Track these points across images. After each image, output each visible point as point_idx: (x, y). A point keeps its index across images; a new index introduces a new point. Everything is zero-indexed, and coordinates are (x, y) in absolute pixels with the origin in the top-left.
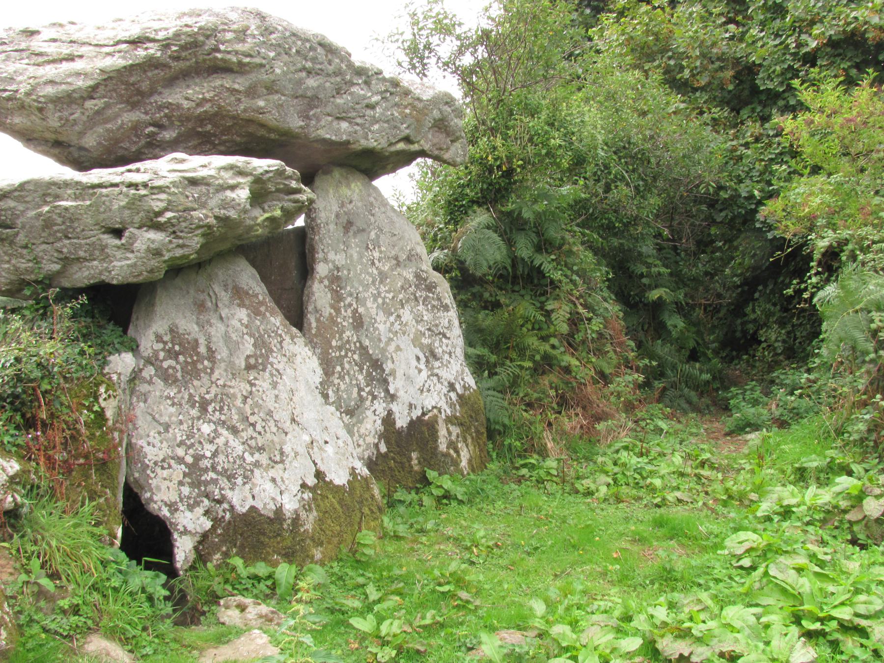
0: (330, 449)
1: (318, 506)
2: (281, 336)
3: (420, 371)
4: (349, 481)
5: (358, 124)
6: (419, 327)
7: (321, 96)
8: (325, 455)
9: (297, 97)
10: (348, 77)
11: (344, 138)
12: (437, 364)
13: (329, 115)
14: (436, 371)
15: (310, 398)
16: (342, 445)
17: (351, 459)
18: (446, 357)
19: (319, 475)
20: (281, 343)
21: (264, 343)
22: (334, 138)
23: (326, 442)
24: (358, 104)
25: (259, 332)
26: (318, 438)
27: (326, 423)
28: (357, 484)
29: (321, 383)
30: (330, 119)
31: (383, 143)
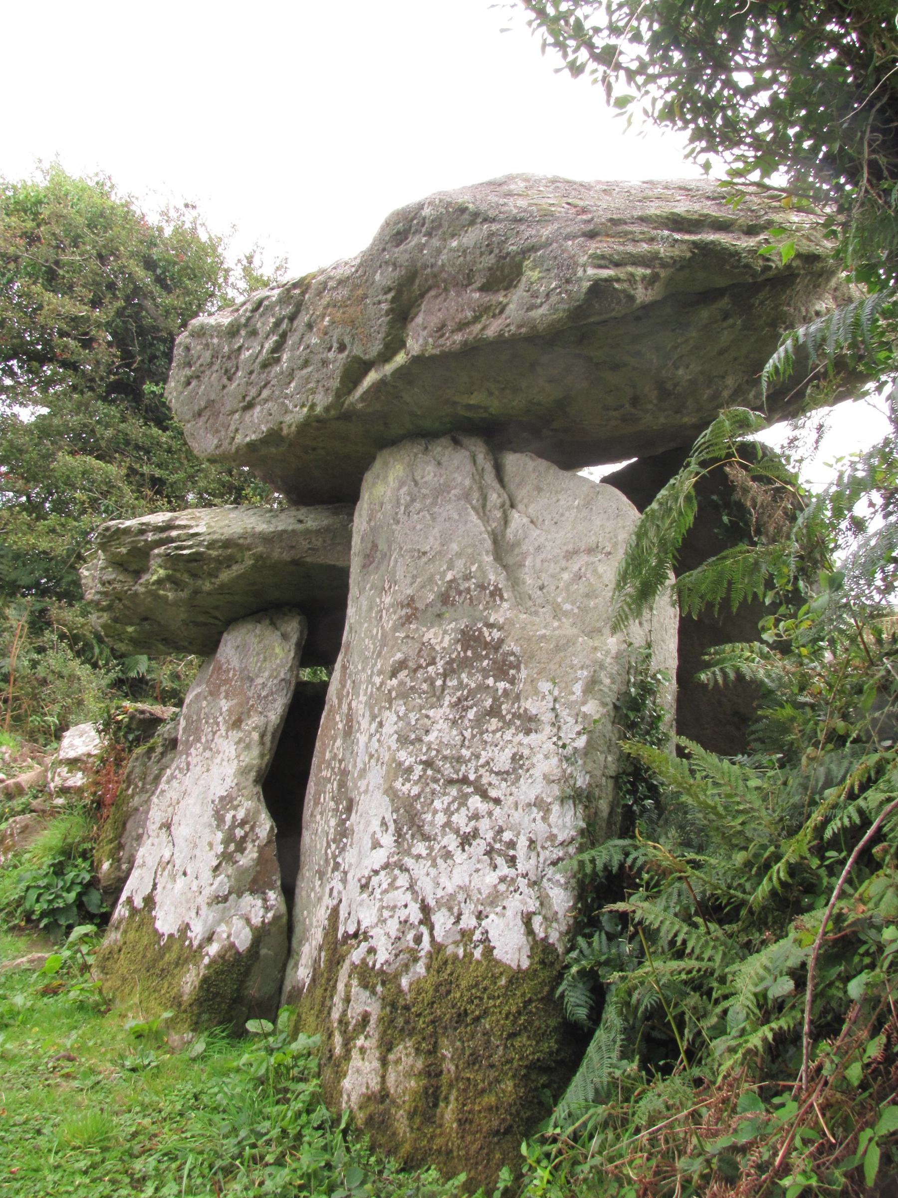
0: (181, 882)
1: (125, 932)
2: (218, 724)
3: (376, 845)
4: (171, 936)
5: (266, 401)
6: (402, 755)
7: (213, 396)
8: (169, 886)
9: (200, 414)
10: (226, 349)
11: (264, 428)
12: (420, 848)
13: (233, 412)
14: (409, 862)
15: (197, 810)
16: (195, 888)
17: (193, 914)
18: (451, 841)
19: (149, 901)
20: (214, 733)
21: (197, 729)
22: (253, 437)
23: (185, 874)
24: (251, 373)
25: (198, 715)
26: (178, 862)
27: (197, 852)
28: (176, 947)
29: (222, 798)
30: (237, 416)
31: (322, 400)
